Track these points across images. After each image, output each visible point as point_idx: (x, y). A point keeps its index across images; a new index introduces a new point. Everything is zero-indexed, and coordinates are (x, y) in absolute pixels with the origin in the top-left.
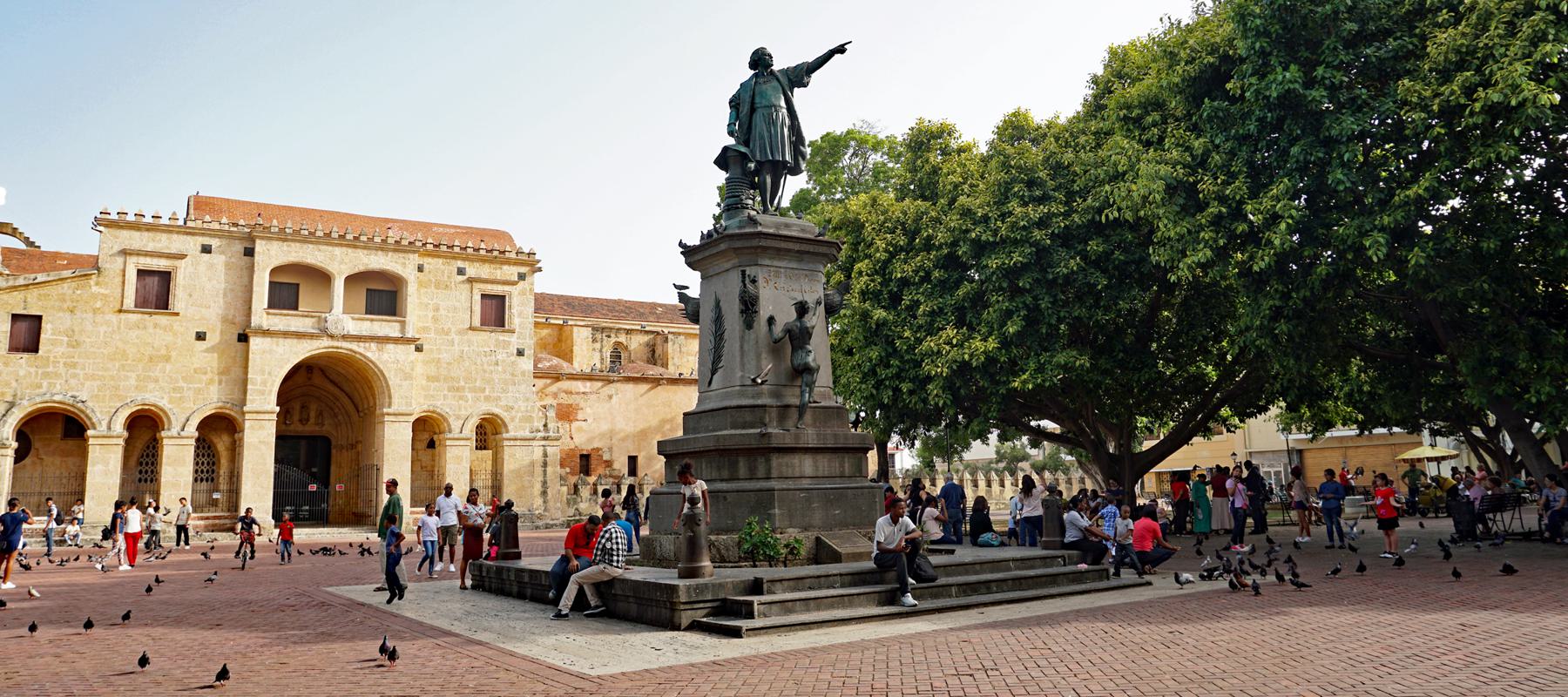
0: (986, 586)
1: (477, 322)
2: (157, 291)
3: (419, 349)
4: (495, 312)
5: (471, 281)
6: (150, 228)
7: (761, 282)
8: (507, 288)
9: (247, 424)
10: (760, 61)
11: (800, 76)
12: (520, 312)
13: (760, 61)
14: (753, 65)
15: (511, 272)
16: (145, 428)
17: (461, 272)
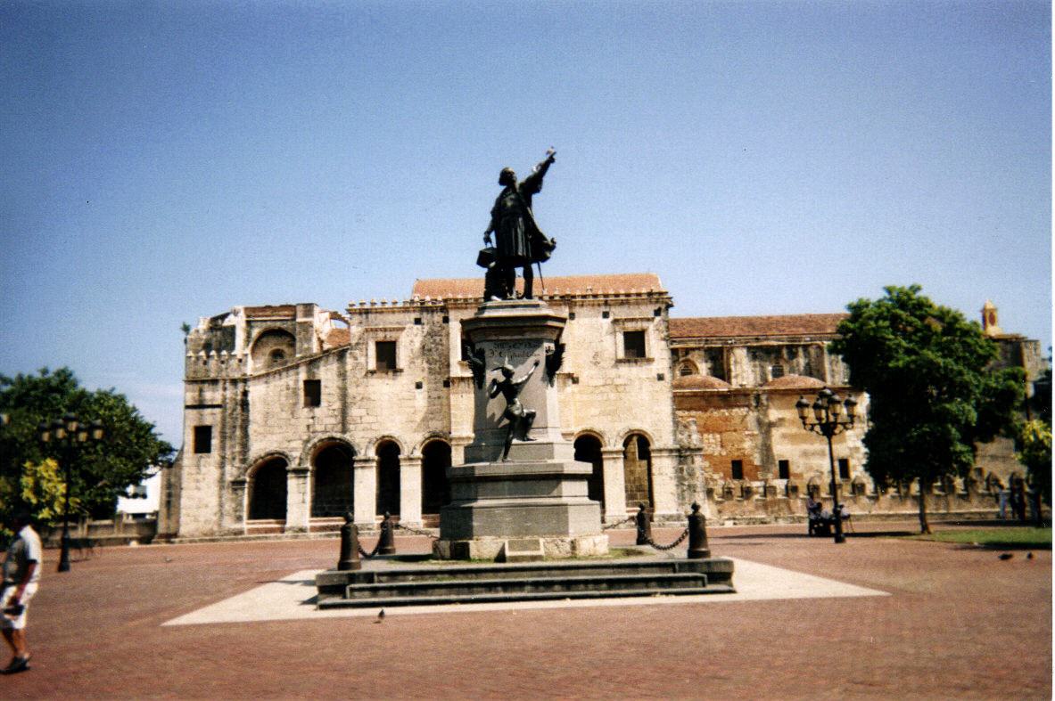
0: (549, 585)
1: (621, 355)
2: (387, 356)
3: (575, 381)
4: (635, 345)
5: (616, 321)
6: (392, 311)
7: (487, 353)
8: (645, 325)
9: (453, 449)
10: (506, 178)
11: (534, 183)
12: (656, 347)
13: (506, 178)
14: (502, 182)
15: (649, 311)
16: (389, 452)
17: (606, 315)
